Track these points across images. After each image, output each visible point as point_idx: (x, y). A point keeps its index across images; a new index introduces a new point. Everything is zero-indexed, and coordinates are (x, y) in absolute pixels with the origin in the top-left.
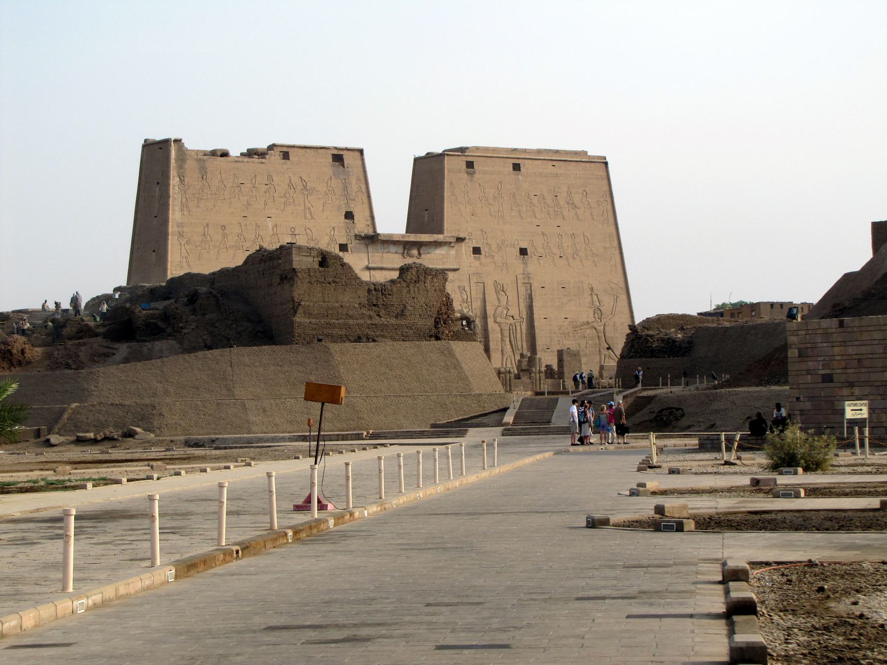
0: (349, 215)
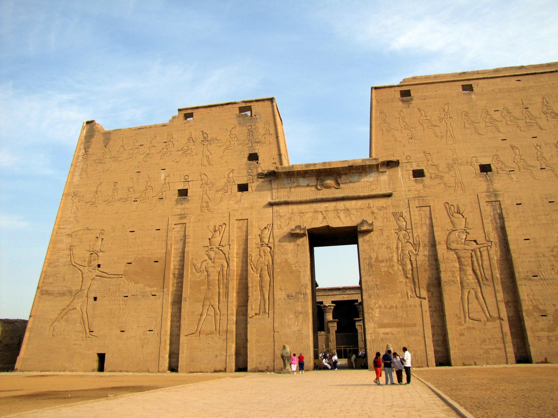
0: (253, 157)
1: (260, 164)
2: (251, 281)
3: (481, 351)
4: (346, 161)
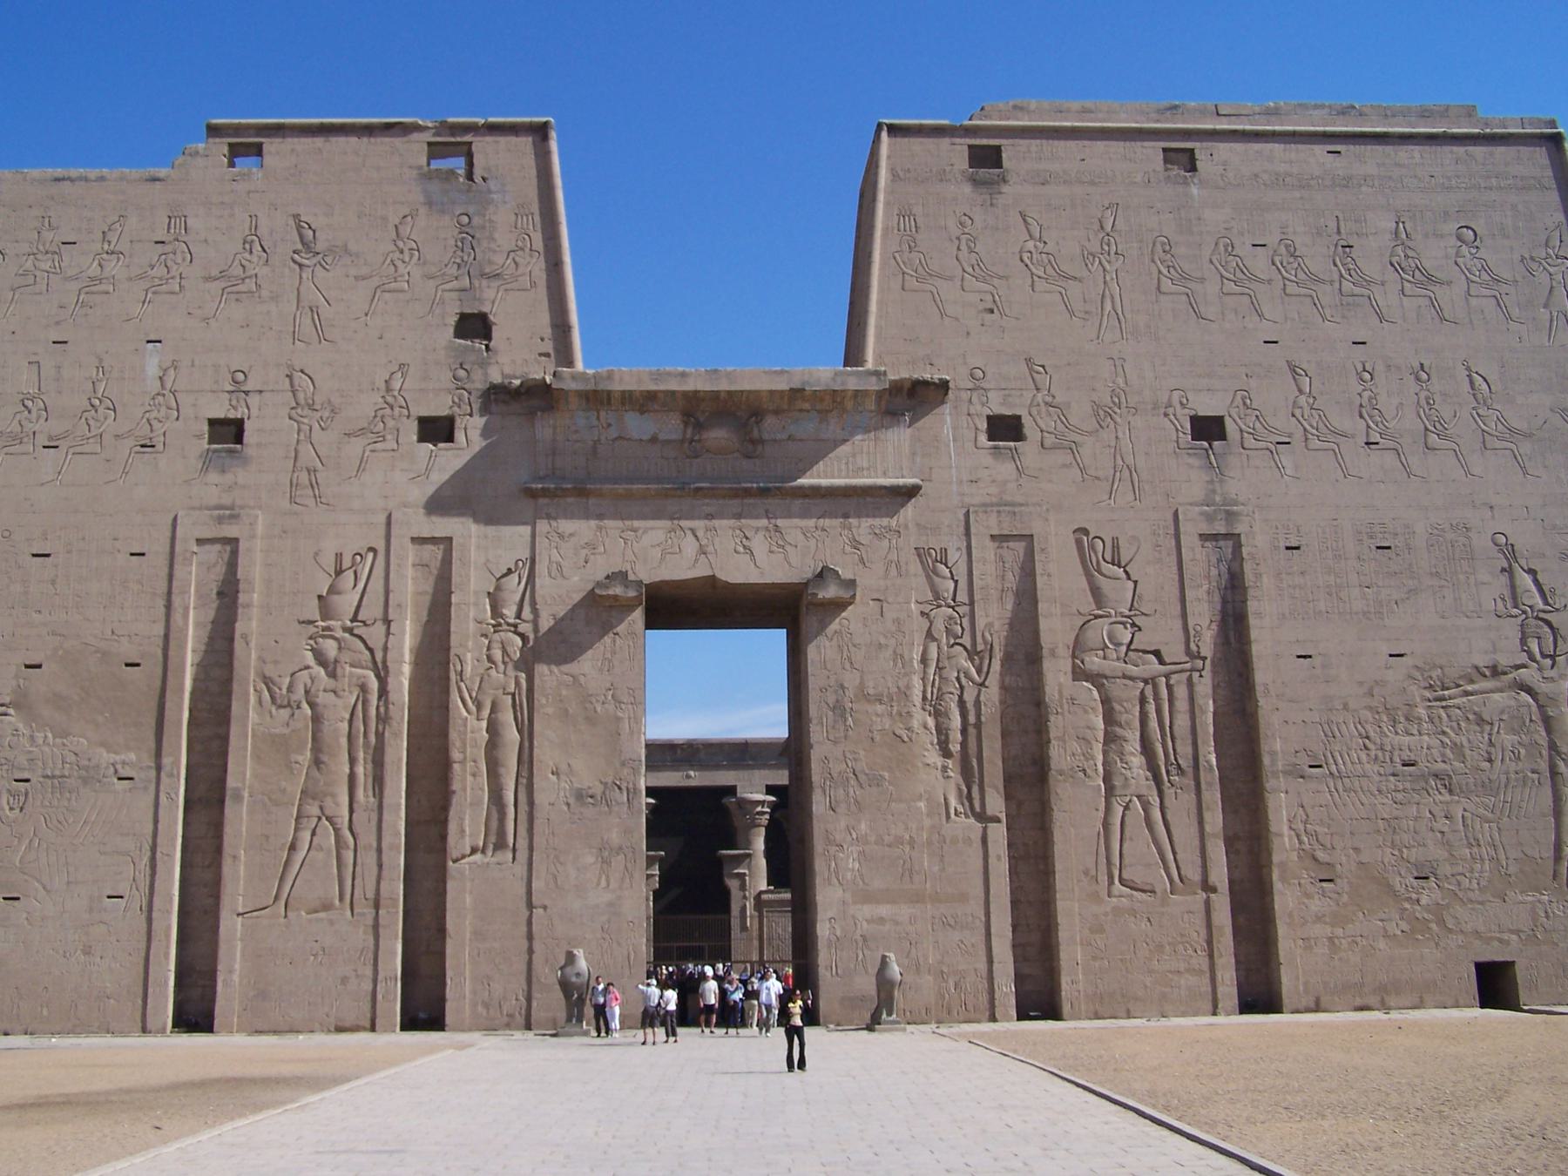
0: (475, 326)
1: (496, 352)
2: (458, 744)
3: (1148, 981)
4: (782, 372)
